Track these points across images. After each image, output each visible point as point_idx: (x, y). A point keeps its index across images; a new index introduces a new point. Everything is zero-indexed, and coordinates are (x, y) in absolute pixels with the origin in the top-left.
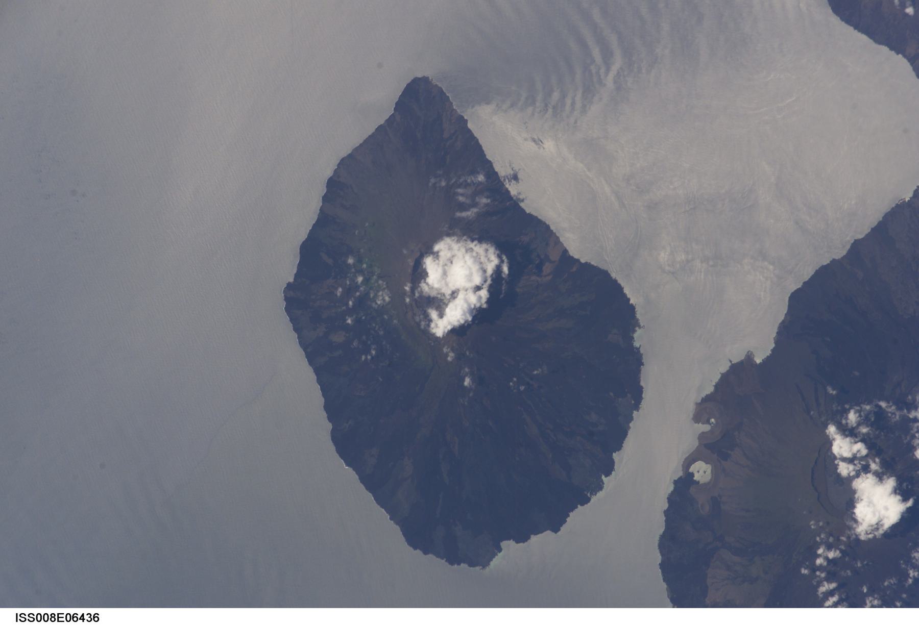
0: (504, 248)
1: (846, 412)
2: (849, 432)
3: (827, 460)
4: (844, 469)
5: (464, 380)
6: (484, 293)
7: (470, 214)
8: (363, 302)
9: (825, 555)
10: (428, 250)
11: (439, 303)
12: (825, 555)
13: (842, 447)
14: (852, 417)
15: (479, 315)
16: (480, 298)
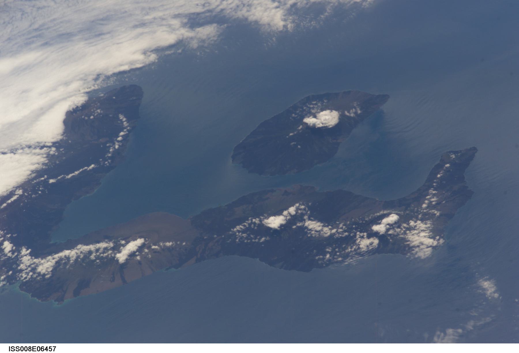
0: (337, 126)
1: (304, 205)
2: (298, 209)
3: (287, 209)
4: (285, 213)
5: (291, 133)
6: (321, 125)
7: (347, 113)
8: (313, 108)
9: (257, 221)
10: (331, 110)
11: (315, 117)
12: (257, 221)
13: (292, 210)
14: (303, 207)
15: (313, 130)
16: (319, 124)
